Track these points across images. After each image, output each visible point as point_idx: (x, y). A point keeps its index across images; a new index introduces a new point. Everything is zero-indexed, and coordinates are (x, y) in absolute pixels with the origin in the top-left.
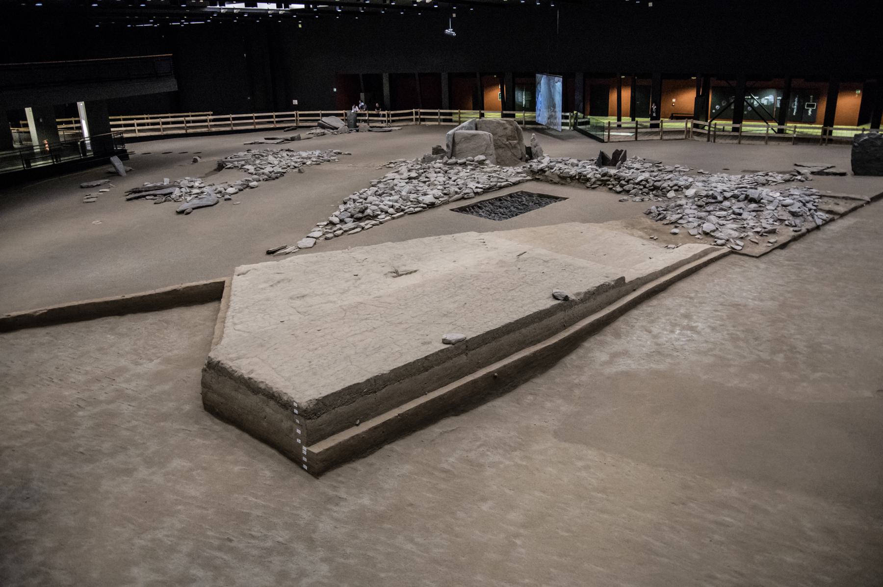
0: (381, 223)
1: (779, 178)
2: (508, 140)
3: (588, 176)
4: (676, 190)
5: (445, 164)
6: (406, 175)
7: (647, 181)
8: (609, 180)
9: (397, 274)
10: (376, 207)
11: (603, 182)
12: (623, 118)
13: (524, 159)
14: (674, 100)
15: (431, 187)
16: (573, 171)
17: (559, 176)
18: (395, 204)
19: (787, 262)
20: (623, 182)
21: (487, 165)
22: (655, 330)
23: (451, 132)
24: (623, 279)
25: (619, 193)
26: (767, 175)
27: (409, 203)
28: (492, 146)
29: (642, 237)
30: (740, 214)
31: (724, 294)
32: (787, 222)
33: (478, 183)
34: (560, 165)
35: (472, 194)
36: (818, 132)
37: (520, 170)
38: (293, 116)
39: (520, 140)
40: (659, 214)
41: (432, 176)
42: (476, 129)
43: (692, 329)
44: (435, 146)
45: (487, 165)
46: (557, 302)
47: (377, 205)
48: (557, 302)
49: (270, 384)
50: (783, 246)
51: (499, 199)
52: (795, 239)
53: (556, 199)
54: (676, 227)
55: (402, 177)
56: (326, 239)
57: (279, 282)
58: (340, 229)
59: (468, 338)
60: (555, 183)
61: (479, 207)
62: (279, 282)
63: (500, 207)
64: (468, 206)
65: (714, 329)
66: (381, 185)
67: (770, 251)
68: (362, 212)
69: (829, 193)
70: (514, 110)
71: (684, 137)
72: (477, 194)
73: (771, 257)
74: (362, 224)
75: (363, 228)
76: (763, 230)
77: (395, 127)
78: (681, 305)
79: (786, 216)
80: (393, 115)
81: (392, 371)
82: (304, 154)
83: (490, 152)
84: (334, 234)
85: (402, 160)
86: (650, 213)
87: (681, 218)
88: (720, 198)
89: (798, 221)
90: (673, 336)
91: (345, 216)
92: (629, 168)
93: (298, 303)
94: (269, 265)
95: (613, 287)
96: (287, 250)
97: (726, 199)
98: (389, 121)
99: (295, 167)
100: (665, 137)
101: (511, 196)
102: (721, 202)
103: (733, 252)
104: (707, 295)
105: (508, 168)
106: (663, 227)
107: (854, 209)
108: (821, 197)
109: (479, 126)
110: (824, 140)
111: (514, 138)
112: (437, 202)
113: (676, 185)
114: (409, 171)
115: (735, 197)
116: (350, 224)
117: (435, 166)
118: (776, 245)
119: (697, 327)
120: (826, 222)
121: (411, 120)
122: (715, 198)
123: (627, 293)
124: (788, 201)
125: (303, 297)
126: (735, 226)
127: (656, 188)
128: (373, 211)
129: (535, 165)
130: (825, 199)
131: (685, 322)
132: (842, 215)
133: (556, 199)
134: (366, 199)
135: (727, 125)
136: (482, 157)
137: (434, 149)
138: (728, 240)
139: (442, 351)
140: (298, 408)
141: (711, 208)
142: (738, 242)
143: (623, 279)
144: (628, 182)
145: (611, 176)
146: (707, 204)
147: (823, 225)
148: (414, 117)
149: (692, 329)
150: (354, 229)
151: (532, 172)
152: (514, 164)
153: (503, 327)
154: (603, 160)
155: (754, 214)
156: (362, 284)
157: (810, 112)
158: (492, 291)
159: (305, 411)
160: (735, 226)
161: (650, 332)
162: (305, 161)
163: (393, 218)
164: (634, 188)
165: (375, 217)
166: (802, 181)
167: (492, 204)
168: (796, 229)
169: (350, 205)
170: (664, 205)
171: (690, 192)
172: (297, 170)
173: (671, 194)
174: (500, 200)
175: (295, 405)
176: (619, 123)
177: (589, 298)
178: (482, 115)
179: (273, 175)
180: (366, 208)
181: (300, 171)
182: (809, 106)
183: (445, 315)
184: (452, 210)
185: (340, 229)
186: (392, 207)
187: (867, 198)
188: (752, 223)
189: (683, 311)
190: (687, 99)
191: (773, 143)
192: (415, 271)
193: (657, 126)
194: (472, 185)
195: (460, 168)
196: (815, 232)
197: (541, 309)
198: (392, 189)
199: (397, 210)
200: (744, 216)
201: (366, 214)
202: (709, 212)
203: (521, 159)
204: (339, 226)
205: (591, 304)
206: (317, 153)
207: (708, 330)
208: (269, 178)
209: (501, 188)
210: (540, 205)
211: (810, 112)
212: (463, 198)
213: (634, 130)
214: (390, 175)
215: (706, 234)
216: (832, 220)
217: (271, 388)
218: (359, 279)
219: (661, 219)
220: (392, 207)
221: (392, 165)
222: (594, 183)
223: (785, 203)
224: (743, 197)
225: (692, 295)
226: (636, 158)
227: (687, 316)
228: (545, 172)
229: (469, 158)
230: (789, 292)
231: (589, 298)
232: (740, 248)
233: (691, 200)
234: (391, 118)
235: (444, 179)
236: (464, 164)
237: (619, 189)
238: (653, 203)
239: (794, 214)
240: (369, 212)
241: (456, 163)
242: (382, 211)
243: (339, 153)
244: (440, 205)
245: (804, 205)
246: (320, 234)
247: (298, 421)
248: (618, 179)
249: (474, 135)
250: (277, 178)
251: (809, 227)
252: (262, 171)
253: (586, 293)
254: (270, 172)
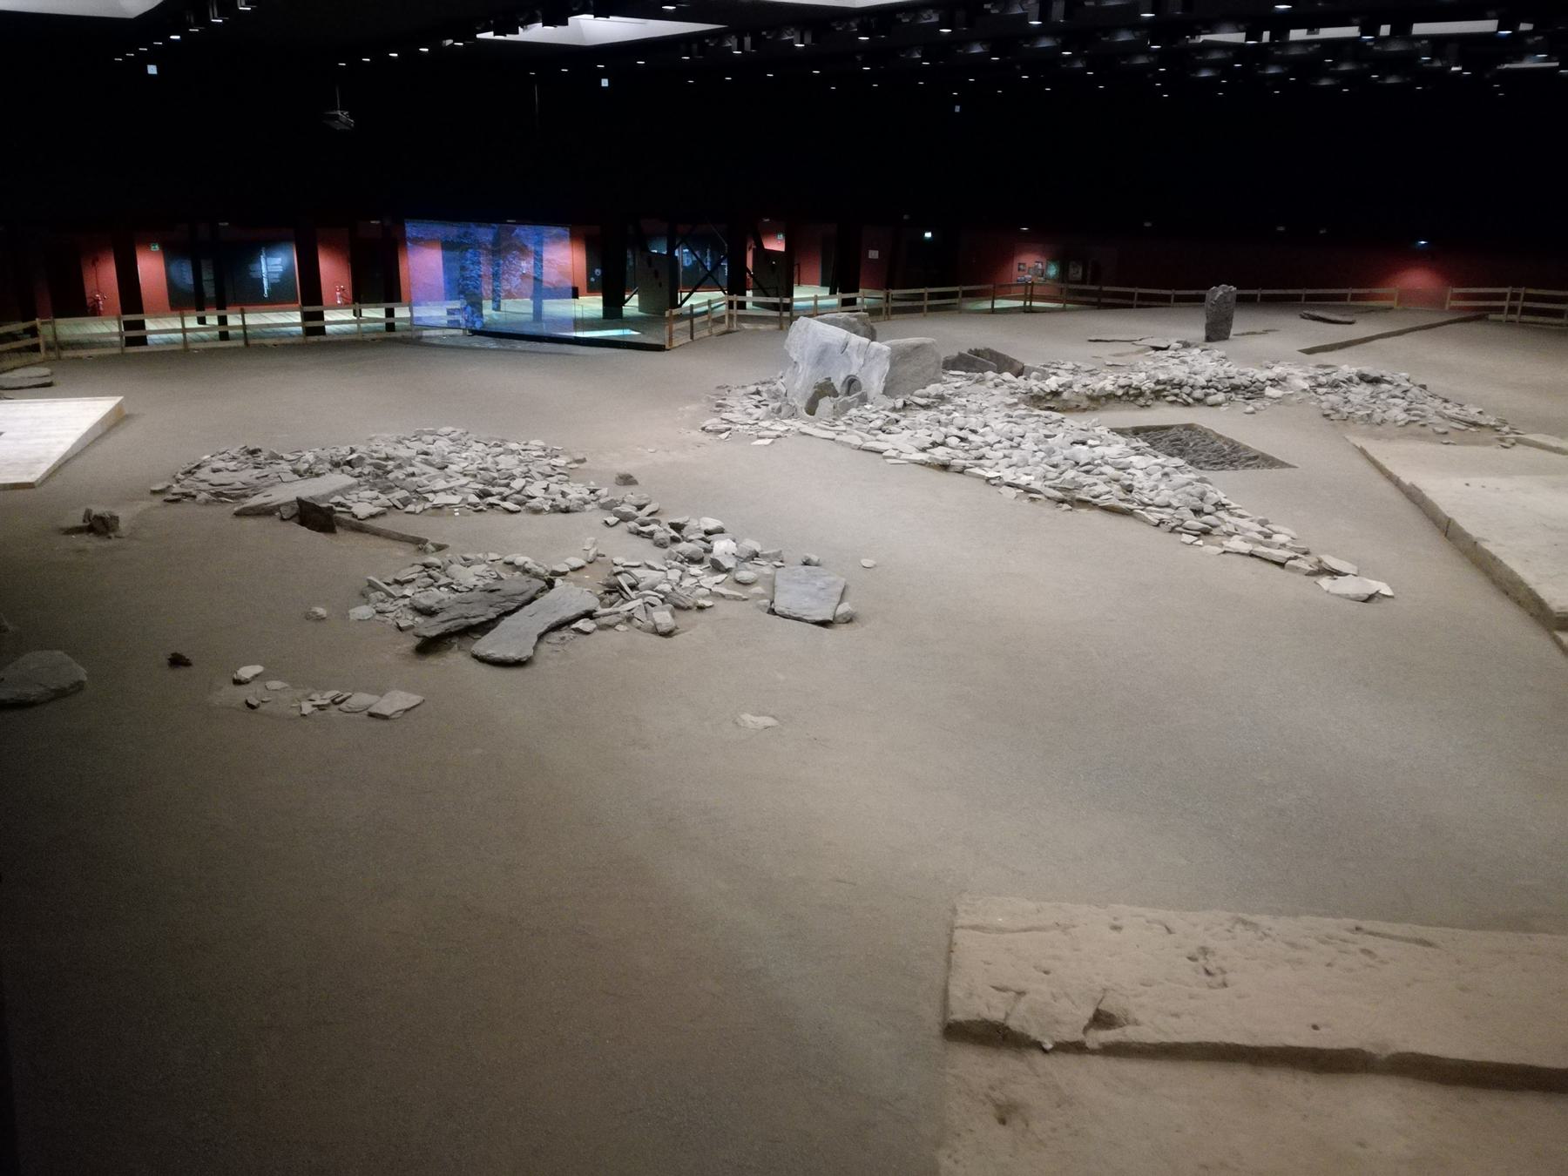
12: (503, 302)
16: (1107, 383)
17: (1091, 398)
115: (1350, 380)
127: (1235, 388)
173: (1269, 391)
176: (390, 320)
248: (1180, 386)
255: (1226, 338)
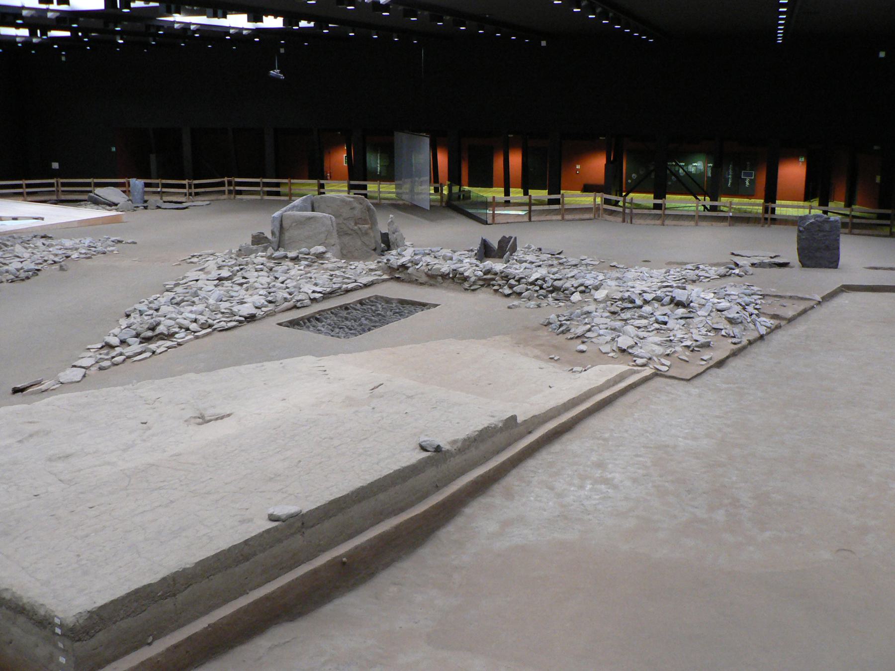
0: (179, 344)
1: (713, 272)
2: (356, 224)
3: (466, 274)
4: (582, 292)
5: (270, 258)
6: (214, 274)
7: (544, 280)
8: (493, 279)
9: (203, 420)
10: (172, 322)
11: (487, 281)
12: (511, 190)
13: (379, 251)
14: (578, 167)
15: (250, 292)
16: (445, 268)
17: (428, 275)
18: (199, 317)
19: (725, 386)
20: (512, 282)
21: (328, 259)
22: (560, 485)
23: (277, 214)
24: (514, 418)
25: (508, 296)
26: (698, 268)
27: (220, 315)
28: (335, 233)
29: (537, 357)
30: (665, 323)
31: (647, 432)
32: (723, 333)
33: (316, 285)
34: (428, 259)
35: (308, 302)
36: (760, 209)
37: (373, 267)
38: (52, 185)
39: (374, 223)
40: (561, 325)
41: (252, 275)
42: (313, 210)
43: (606, 481)
44: (255, 232)
45: (328, 259)
46: (425, 455)
47: (174, 319)
48: (425, 455)
49: (19, 593)
50: (720, 364)
51: (346, 307)
52: (734, 354)
53: (423, 306)
54: (583, 342)
55: (210, 277)
56: (101, 369)
57: (31, 436)
58: (121, 354)
59: (304, 511)
60: (421, 284)
61: (317, 319)
62: (31, 436)
63: (347, 319)
64: (302, 319)
65: (635, 480)
66: (179, 289)
67: (704, 372)
68: (153, 329)
69: (773, 290)
70: (365, 180)
71: (592, 216)
72: (314, 300)
73: (706, 378)
74: (153, 346)
75: (154, 352)
76: (695, 344)
77: (200, 201)
78: (592, 450)
79: (723, 324)
80: (197, 186)
81: (198, 564)
82: (68, 243)
83: (332, 241)
84: (112, 360)
85: (210, 251)
86: (549, 324)
87: (589, 330)
88: (639, 302)
89: (737, 330)
90: (582, 493)
91: (127, 335)
92: (521, 262)
93: (60, 466)
94: (19, 407)
95: (501, 430)
96: (43, 387)
97: (646, 302)
98: (190, 194)
99: (55, 262)
100: (567, 217)
101: (361, 302)
102: (641, 307)
103: (657, 374)
104: (626, 435)
105: (356, 263)
106: (565, 340)
107: (804, 312)
108: (764, 296)
109: (316, 205)
110: (766, 219)
111: (365, 222)
112: (259, 313)
113: (582, 285)
114: (219, 268)
115: (658, 299)
116: (135, 346)
117: (256, 261)
118: (712, 363)
119: (613, 479)
120: (772, 330)
121: (223, 192)
122: (633, 302)
123: (521, 437)
124: (724, 304)
125: (67, 457)
126: (658, 339)
127: (555, 289)
128: (169, 327)
129: (394, 258)
130: (770, 300)
131: (598, 473)
132: (790, 320)
133: (423, 306)
134: (157, 310)
135: (646, 199)
136: (321, 249)
137: (253, 237)
138: (650, 359)
139: (268, 531)
140: (61, 626)
141: (626, 315)
142: (663, 361)
143: (514, 418)
144: (519, 281)
145: (496, 274)
146: (622, 309)
147: (768, 334)
148: (226, 188)
149: (606, 481)
150: (140, 353)
151: (391, 269)
152: (364, 257)
153: (353, 493)
154: (486, 251)
155: (683, 322)
156: (153, 435)
157: (747, 183)
158: (336, 442)
159: (72, 630)
160: (658, 339)
161: (552, 488)
162: (69, 253)
163: (197, 337)
164: (527, 290)
165: (170, 336)
166: (741, 276)
167: (336, 315)
168: (734, 340)
169: (135, 319)
170: (566, 313)
171: (600, 294)
172: (57, 266)
173: (576, 297)
174: (347, 309)
175: (57, 621)
176: (507, 198)
177: (469, 446)
178: (322, 186)
179: (22, 275)
180: (158, 324)
181: (62, 269)
182: (746, 174)
183: (271, 479)
184: (280, 324)
185: (121, 354)
186: (195, 321)
187: (819, 298)
188: (680, 335)
189: (594, 458)
190: (596, 166)
191: (704, 223)
192: (229, 415)
193: (557, 201)
194: (308, 288)
195: (291, 264)
196: (759, 343)
197: (404, 465)
198: (196, 295)
199: (203, 326)
200: (668, 326)
201: (157, 331)
202: (626, 320)
203: (375, 250)
204: (118, 350)
205: (473, 453)
206: (87, 241)
207: (628, 483)
208: (16, 279)
209: (347, 291)
210: (401, 315)
211: (747, 183)
212: (295, 307)
213: (527, 208)
214: (192, 274)
215: (623, 351)
216: (778, 327)
217: (21, 598)
218: (149, 428)
219: (563, 332)
220: (195, 321)
221: (195, 260)
222: (474, 283)
223: (720, 306)
224: (667, 299)
225: (607, 435)
226: (529, 247)
227: (600, 465)
228: (407, 268)
229: (303, 250)
230: (729, 426)
231: (469, 446)
232: (666, 368)
233: (602, 305)
234: (193, 190)
235: (269, 280)
236: (295, 259)
237: (507, 291)
238: (552, 309)
239: (731, 321)
240: (161, 329)
241: (286, 257)
242: (181, 328)
243: (120, 242)
244: (263, 317)
245: (744, 309)
246: (91, 361)
247: (61, 645)
248: (506, 278)
249: (310, 218)
250: (28, 278)
251: (751, 338)
252: (6, 267)
253: (465, 440)
254: (18, 270)
255: (836, 267)
